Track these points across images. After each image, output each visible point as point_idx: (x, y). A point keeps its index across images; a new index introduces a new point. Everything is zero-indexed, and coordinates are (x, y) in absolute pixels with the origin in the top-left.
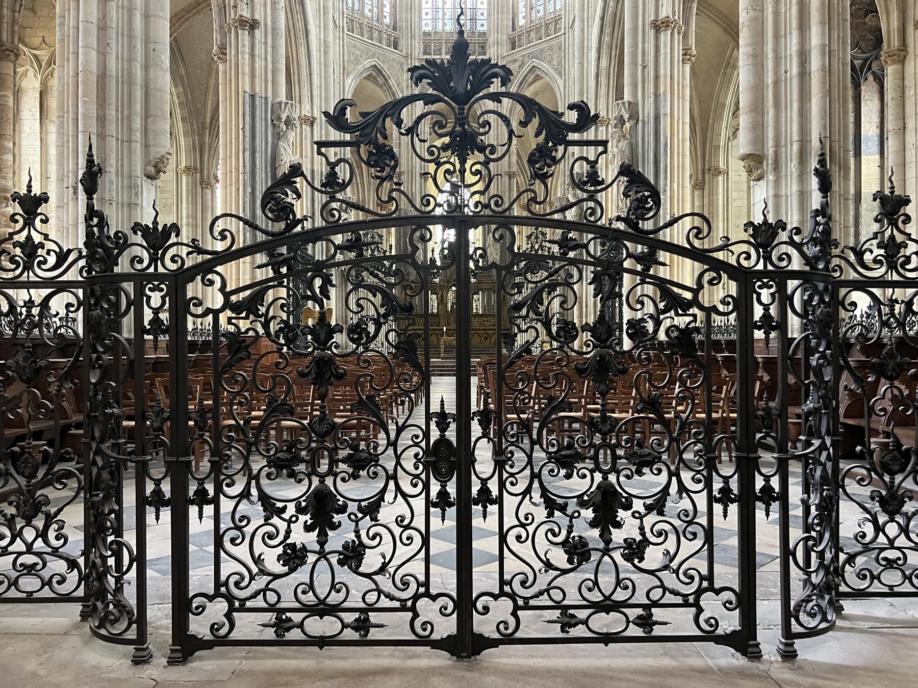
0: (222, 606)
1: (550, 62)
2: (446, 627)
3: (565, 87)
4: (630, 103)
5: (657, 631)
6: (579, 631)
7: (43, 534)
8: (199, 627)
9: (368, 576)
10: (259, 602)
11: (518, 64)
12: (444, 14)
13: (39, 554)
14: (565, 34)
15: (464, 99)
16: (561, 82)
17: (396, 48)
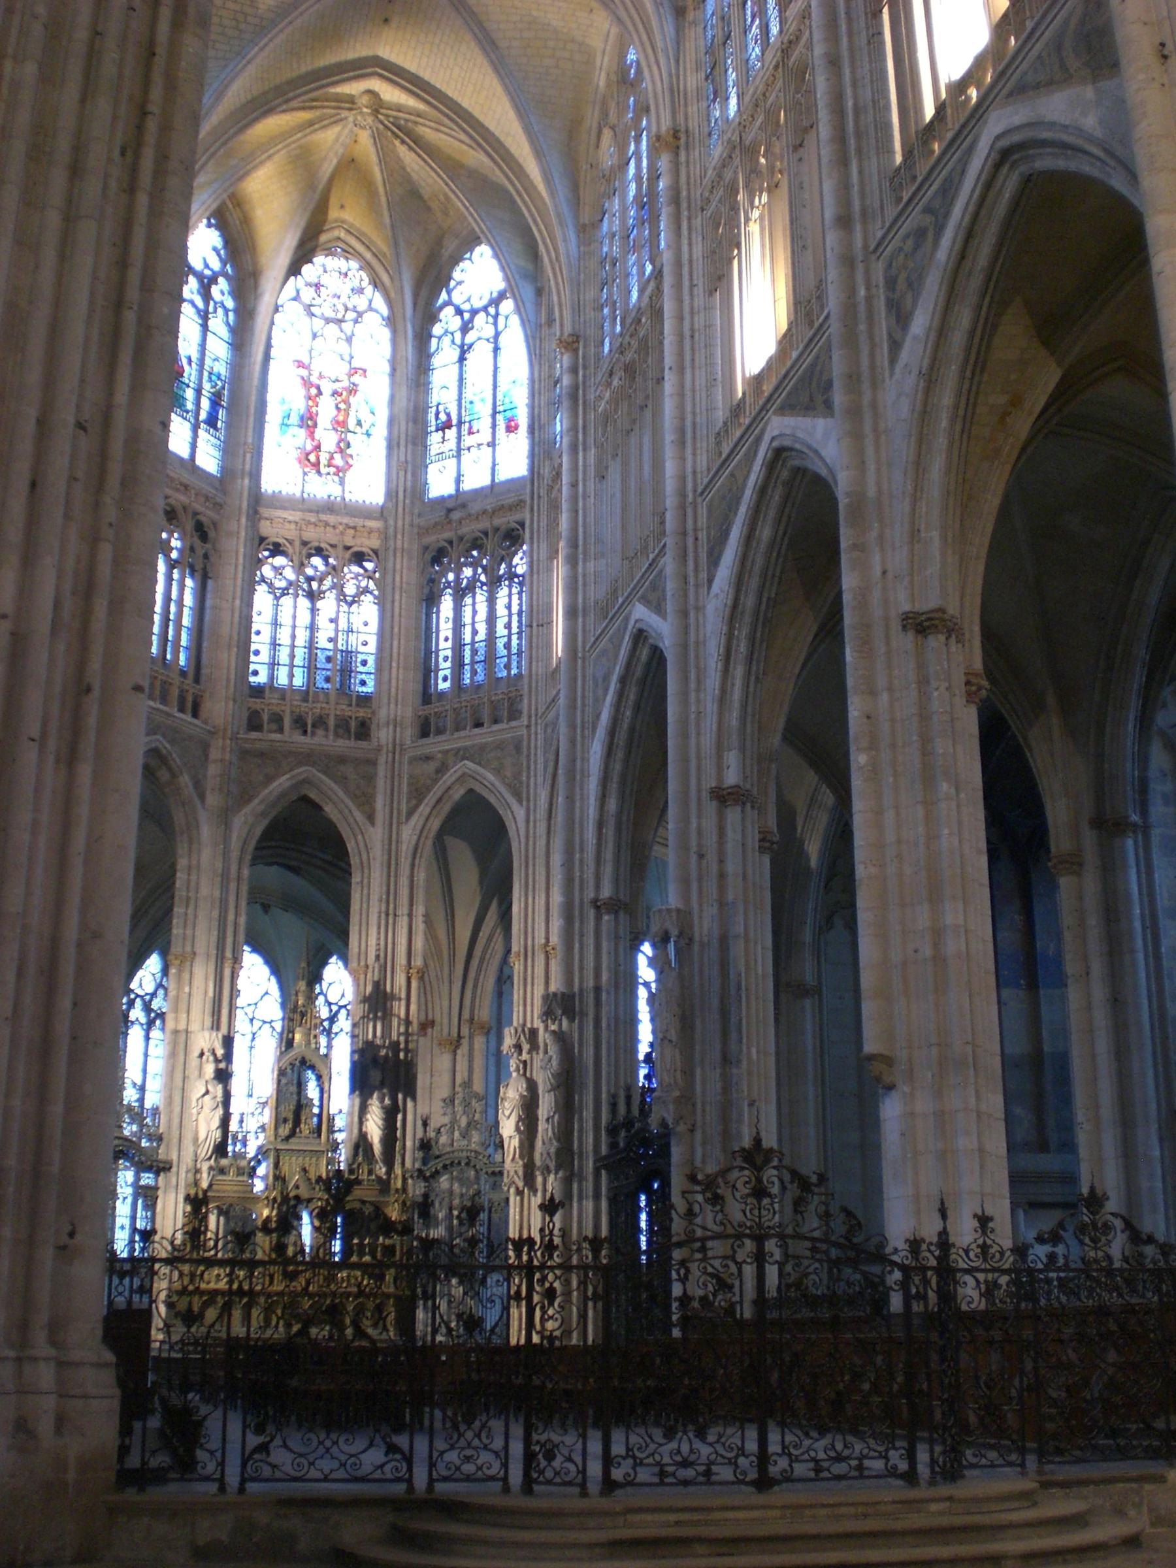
0: (630, 1461)
1: (498, 772)
2: (753, 1475)
3: (528, 821)
4: (678, 911)
5: (866, 1473)
6: (825, 1474)
7: (478, 1436)
8: (617, 1474)
9: (711, 1444)
10: (650, 1460)
11: (431, 767)
12: (292, 656)
13: (475, 1448)
14: (528, 726)
15: (758, 1169)
16: (520, 813)
17: (195, 715)
